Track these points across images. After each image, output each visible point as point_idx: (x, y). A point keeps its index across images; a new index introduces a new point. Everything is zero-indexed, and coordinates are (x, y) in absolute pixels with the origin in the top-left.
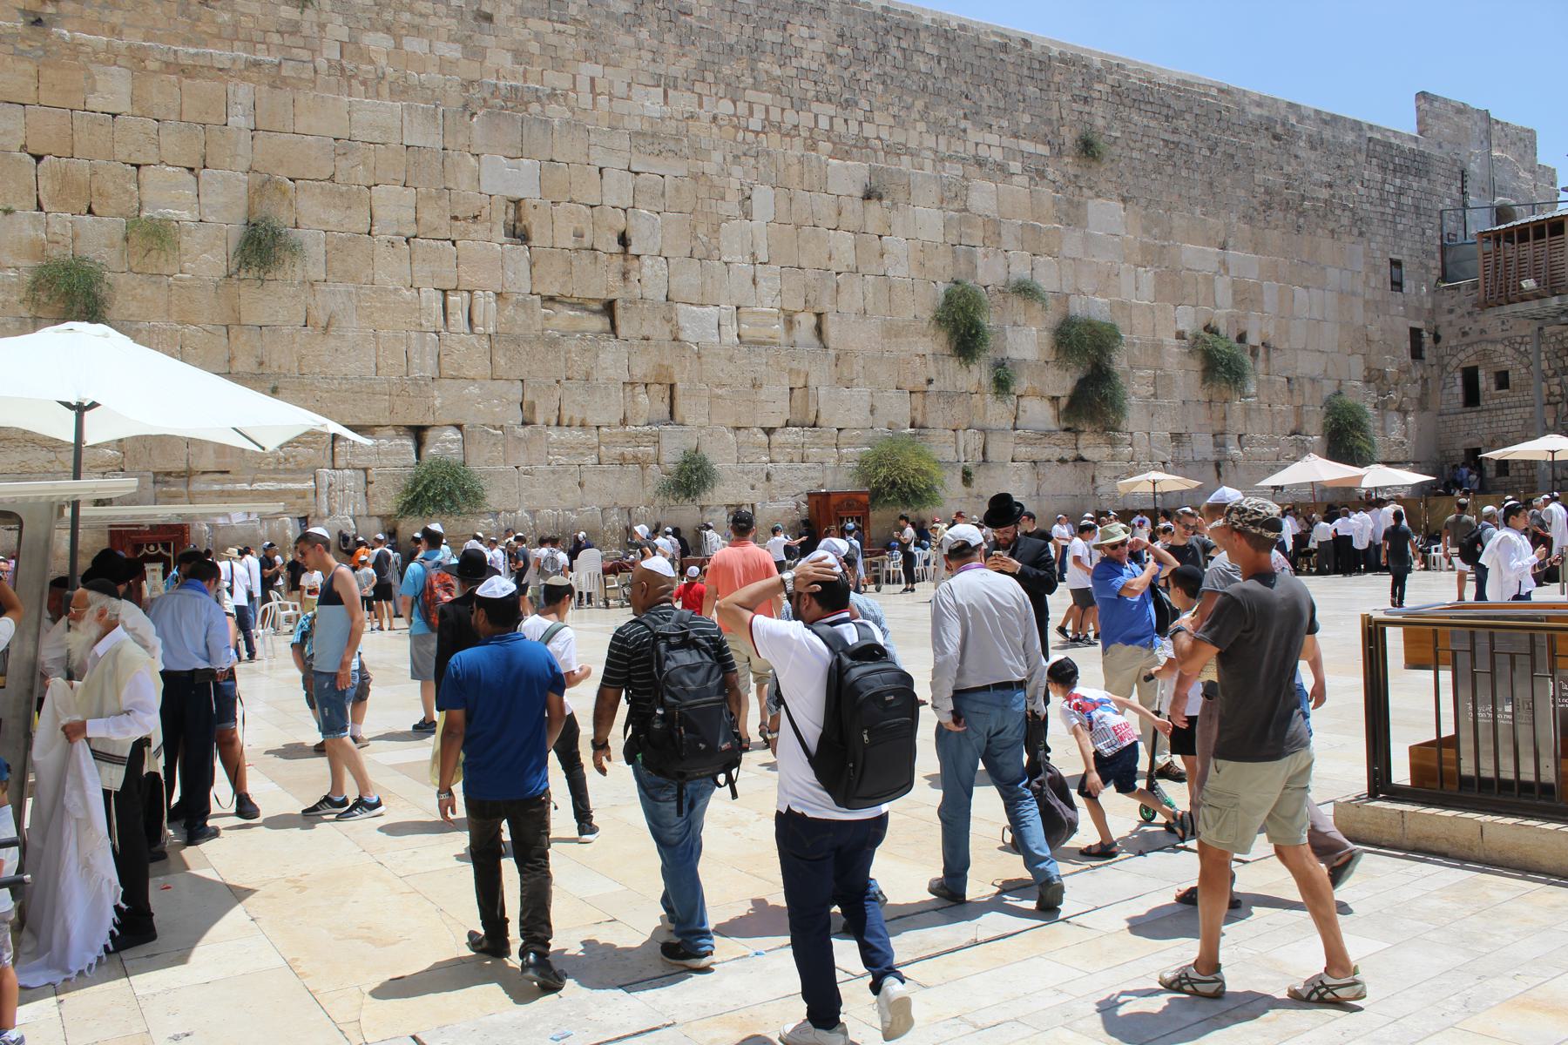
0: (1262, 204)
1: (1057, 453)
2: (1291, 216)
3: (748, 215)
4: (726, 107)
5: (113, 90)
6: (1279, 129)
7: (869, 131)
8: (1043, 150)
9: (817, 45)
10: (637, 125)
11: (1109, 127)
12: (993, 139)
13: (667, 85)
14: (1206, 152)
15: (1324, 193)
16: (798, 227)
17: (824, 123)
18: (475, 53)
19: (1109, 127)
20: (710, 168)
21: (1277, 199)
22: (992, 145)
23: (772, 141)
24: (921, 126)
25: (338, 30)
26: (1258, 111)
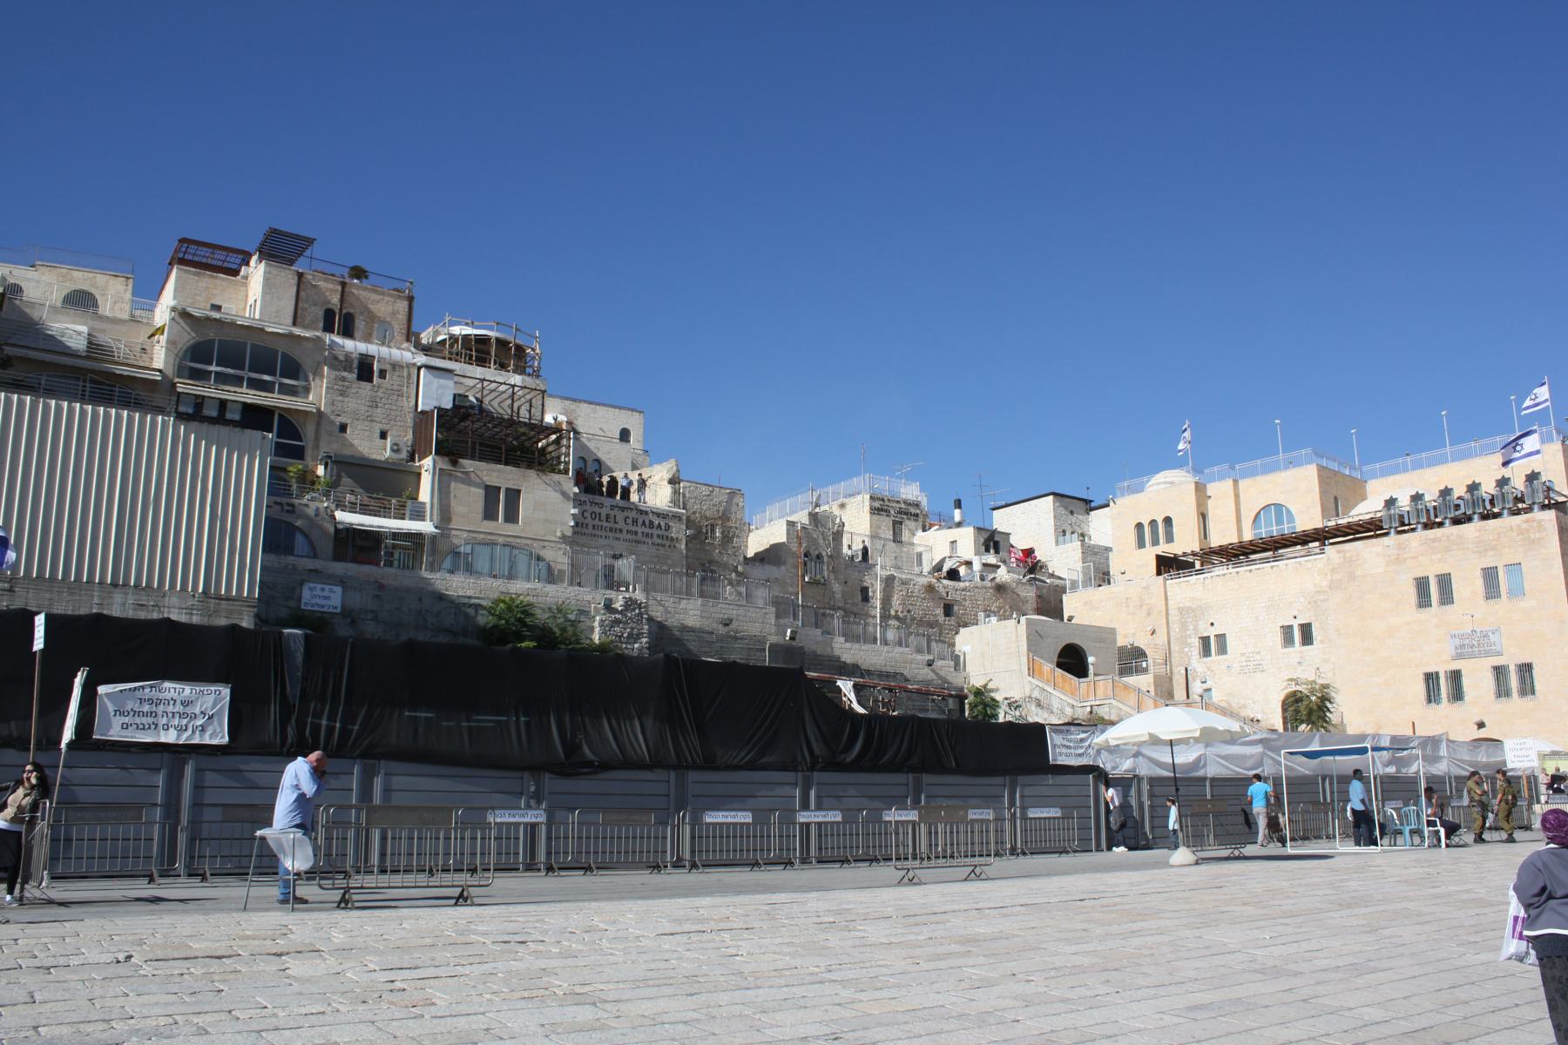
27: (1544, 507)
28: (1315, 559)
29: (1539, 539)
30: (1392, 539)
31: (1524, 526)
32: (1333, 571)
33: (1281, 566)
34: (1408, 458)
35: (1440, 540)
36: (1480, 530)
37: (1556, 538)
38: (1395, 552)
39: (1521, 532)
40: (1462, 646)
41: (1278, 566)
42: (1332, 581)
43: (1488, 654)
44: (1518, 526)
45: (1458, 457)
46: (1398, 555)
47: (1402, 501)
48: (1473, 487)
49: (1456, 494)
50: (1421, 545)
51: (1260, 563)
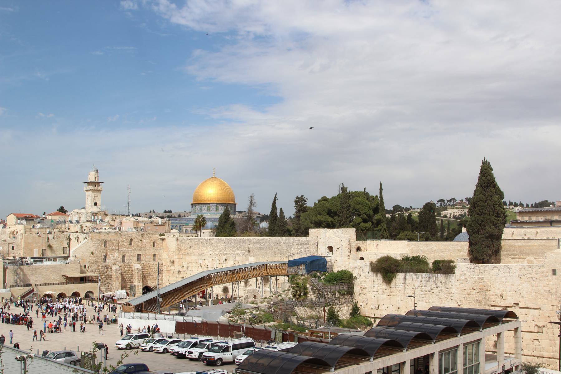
0: (274, 254)
1: (243, 288)
2: (279, 255)
3: (216, 263)
4: (215, 252)
5: (182, 257)
6: (278, 242)
7: (227, 253)
8: (245, 251)
9: (223, 244)
10: (209, 255)
11: (252, 247)
12: (239, 251)
13: (211, 251)
14: (265, 248)
15: (286, 250)
16: (220, 264)
17: (223, 253)
18: (199, 251)
19: (252, 247)
20: (213, 259)
21: (276, 253)
22: (238, 252)
23: (219, 255)
24: (232, 251)
25: (192, 250)
26: (275, 240)
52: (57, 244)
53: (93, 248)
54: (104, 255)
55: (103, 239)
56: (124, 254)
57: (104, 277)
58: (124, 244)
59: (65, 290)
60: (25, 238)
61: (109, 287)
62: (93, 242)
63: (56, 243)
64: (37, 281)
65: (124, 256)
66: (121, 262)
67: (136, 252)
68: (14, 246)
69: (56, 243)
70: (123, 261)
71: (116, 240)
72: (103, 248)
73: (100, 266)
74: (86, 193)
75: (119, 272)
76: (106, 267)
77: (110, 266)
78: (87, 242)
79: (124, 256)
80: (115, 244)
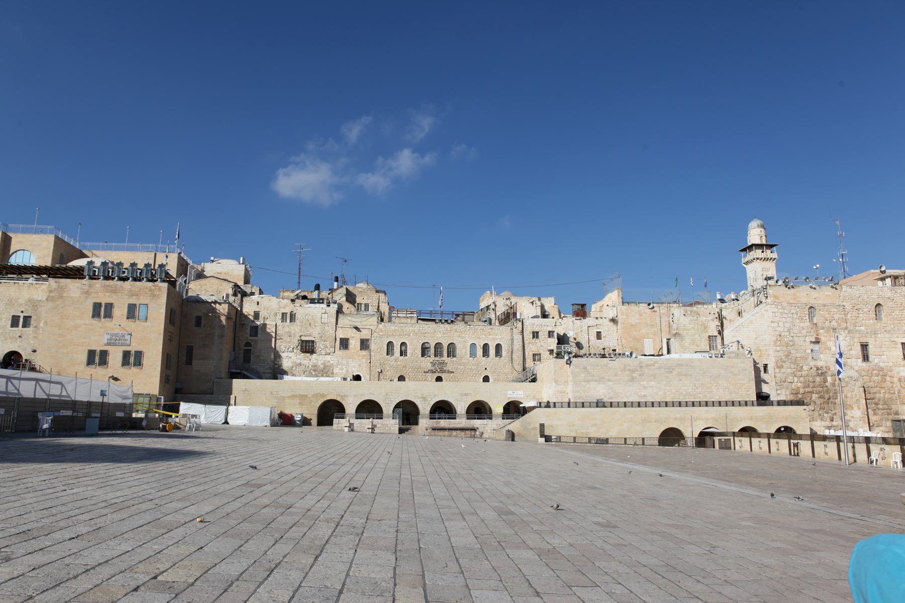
27: (164, 281)
28: (42, 284)
29: (158, 295)
30: (86, 281)
31: (153, 288)
32: (51, 291)
33: (20, 284)
34: (106, 244)
35: (112, 287)
36: (132, 286)
37: (166, 296)
38: (87, 288)
39: (151, 290)
40: (111, 339)
41: (18, 283)
42: (49, 296)
43: (122, 345)
44: (150, 287)
45: (128, 249)
46: (88, 289)
47: (97, 264)
48: (133, 265)
49: (125, 266)
50: (102, 287)
51: (8, 280)
52: (693, 328)
53: (781, 324)
54: (811, 342)
55: (804, 302)
56: (864, 340)
57: (817, 395)
58: (861, 315)
59: (716, 421)
60: (623, 315)
61: (835, 423)
62: (780, 311)
63: (691, 326)
64: (645, 396)
65: (864, 346)
66: (860, 360)
67: (898, 337)
68: (600, 332)
69: (691, 326)
70: (866, 358)
71: (839, 306)
72: (808, 324)
73: (805, 368)
74: (745, 268)
75: (859, 384)
76: (820, 372)
77: (829, 369)
78: (765, 308)
79: (864, 346)
80: (836, 316)
